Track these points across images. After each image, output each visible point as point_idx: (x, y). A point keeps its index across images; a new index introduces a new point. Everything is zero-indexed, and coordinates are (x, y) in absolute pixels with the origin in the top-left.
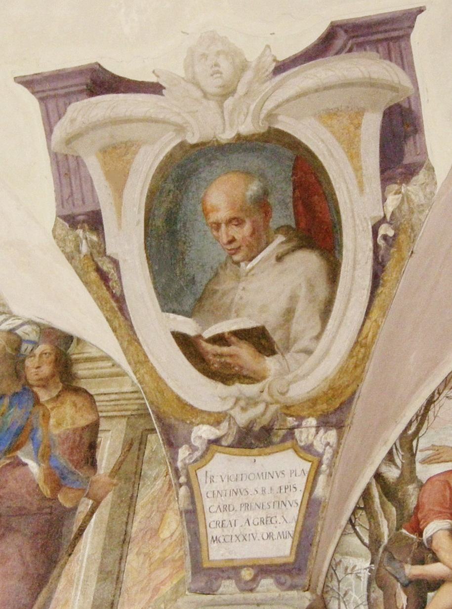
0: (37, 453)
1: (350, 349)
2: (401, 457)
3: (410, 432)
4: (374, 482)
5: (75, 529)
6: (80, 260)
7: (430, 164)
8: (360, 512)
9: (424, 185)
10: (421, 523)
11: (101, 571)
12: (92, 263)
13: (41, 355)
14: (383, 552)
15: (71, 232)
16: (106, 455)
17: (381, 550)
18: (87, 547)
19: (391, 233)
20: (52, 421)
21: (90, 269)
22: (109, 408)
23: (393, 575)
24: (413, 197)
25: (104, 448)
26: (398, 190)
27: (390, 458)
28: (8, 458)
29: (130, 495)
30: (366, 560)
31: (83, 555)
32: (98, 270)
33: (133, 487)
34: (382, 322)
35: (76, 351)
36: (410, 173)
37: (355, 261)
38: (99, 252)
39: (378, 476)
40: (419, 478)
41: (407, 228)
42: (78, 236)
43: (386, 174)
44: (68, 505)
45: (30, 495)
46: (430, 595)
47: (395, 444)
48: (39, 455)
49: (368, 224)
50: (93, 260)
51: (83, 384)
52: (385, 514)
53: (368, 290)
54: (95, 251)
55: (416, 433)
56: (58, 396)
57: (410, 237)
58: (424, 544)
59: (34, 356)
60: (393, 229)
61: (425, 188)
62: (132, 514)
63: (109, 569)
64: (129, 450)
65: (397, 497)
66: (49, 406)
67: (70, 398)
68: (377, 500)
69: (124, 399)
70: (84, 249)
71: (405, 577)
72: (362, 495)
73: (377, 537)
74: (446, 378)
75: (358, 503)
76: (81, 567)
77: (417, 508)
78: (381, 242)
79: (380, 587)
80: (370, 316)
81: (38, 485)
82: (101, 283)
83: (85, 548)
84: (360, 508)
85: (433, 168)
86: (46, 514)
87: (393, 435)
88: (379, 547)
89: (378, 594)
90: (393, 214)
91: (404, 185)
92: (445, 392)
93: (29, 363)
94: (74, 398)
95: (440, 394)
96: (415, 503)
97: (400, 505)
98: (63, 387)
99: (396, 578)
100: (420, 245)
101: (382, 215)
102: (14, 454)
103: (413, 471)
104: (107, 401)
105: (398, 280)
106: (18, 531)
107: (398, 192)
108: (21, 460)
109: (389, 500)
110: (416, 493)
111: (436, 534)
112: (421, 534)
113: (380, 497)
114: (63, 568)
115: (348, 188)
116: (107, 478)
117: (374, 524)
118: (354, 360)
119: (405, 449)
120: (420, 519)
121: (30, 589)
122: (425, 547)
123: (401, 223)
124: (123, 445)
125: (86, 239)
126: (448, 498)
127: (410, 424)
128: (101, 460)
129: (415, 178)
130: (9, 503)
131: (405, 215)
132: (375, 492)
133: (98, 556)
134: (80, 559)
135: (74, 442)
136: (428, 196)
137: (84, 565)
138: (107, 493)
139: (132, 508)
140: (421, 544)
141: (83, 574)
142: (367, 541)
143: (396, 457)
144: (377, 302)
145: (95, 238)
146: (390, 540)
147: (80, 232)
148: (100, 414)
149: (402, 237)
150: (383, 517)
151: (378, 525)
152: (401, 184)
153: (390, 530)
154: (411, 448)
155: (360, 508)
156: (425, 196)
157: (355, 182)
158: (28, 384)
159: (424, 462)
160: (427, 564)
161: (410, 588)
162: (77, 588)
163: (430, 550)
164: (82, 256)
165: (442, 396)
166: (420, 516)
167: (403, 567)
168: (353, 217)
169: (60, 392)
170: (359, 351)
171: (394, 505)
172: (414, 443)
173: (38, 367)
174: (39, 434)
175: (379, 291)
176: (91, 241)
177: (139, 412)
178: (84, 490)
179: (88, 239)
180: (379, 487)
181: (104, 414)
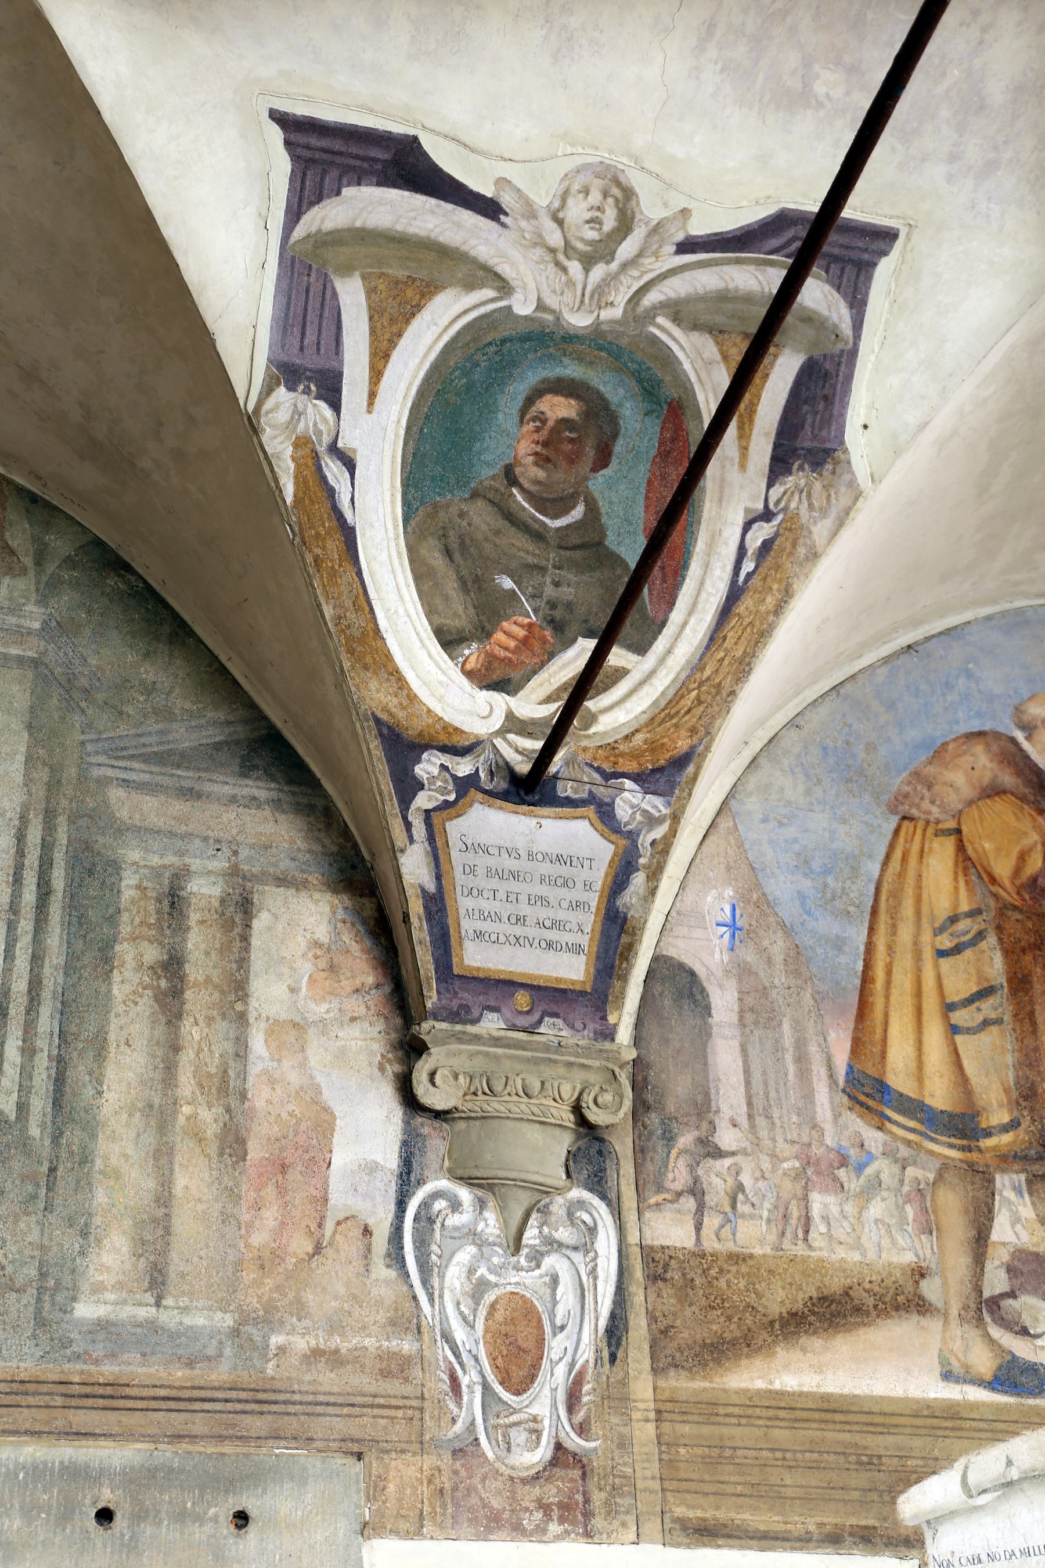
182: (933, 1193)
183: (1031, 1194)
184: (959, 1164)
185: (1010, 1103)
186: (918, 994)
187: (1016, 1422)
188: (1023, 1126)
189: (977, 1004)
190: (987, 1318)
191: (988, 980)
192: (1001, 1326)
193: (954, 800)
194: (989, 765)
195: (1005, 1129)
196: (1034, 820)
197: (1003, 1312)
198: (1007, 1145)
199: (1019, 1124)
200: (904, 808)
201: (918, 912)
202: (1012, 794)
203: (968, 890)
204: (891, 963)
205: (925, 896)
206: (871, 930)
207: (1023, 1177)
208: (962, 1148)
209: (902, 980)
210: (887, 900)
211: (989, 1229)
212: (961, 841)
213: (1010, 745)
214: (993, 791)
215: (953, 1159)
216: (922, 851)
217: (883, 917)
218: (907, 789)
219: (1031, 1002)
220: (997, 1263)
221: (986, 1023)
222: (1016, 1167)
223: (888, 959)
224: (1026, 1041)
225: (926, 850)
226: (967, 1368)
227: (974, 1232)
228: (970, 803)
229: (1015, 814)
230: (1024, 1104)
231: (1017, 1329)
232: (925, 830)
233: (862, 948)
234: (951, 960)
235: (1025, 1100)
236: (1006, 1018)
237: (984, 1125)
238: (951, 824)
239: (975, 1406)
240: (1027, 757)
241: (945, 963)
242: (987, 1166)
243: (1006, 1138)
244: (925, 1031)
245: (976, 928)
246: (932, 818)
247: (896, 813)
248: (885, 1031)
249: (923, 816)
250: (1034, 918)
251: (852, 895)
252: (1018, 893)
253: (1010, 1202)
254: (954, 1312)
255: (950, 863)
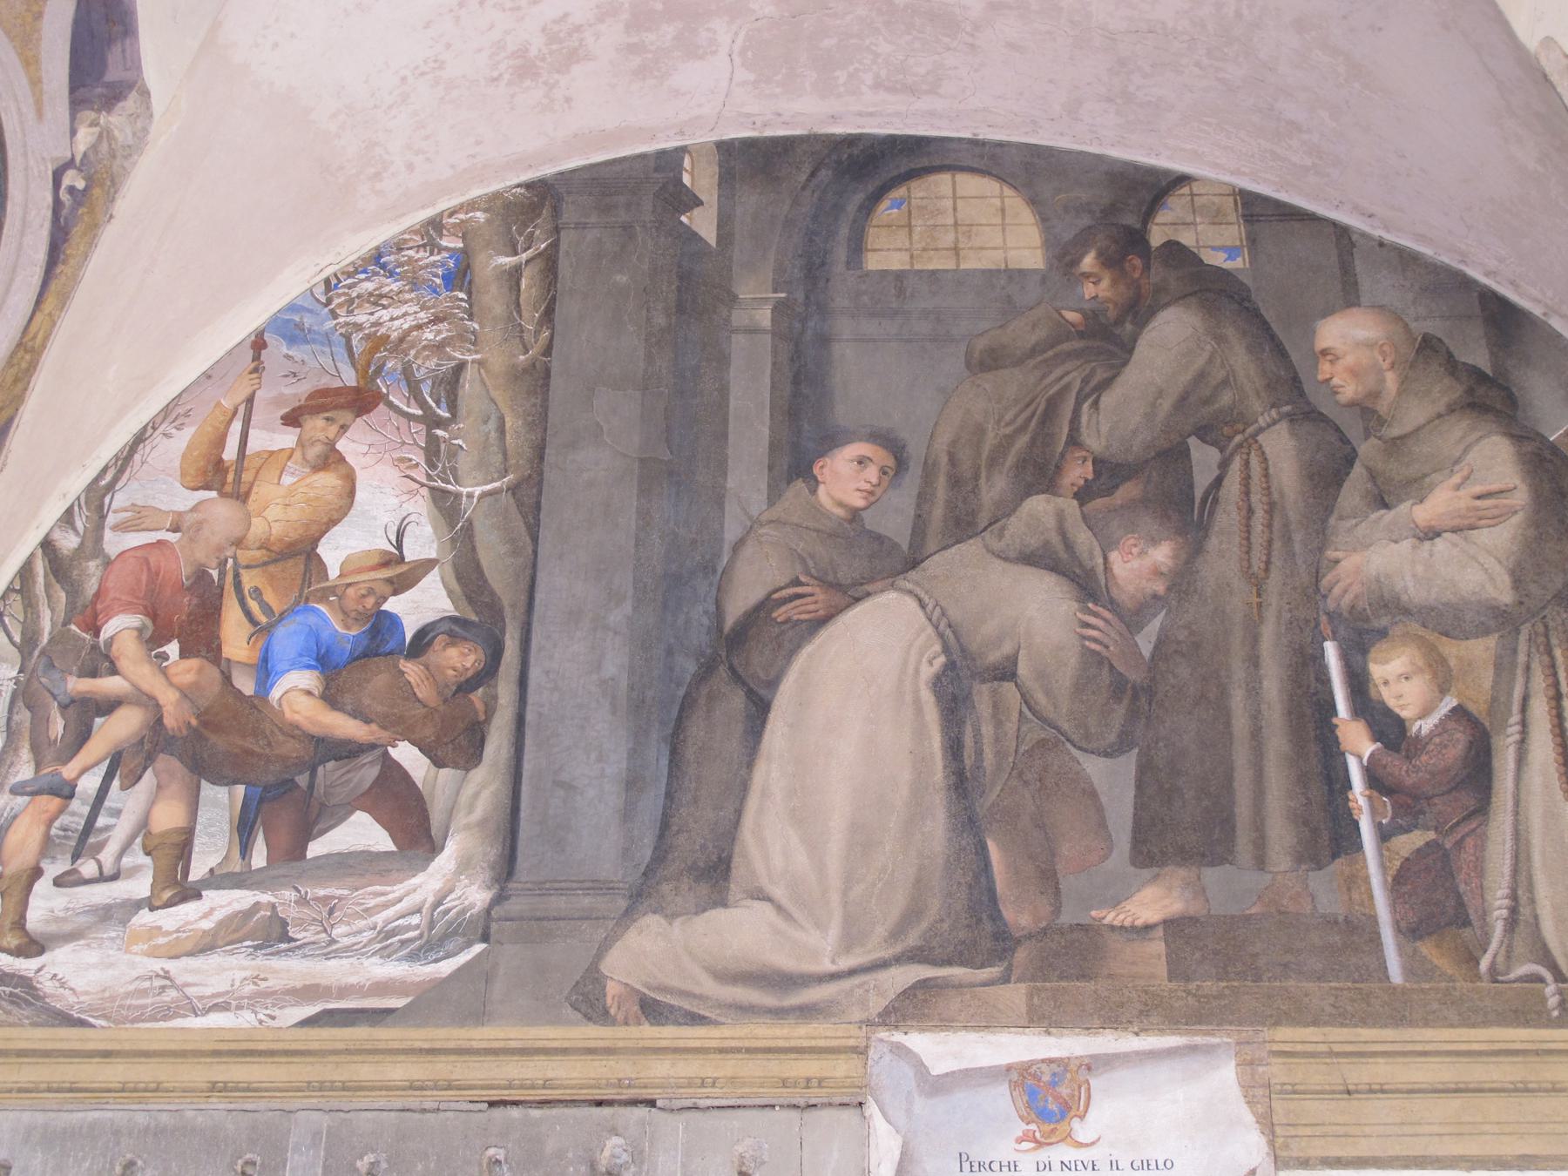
1: (9, 353)
2: (84, 520)
3: (103, 483)
4: (40, 551)
7: (144, 85)
8: (14, 596)
9: (134, 117)
10: (101, 616)
14: (39, 657)
17: (36, 653)
19: (80, 185)
23: (49, 691)
24: (116, 133)
26: (94, 120)
27: (68, 518)
30: (13, 667)
34: (59, 317)
36: (114, 96)
37: (25, 223)
39: (47, 545)
40: (106, 551)
41: (104, 179)
43: (77, 94)
46: (98, 721)
47: (78, 498)
49: (46, 167)
52: (49, 601)
53: (41, 267)
55: (111, 487)
57: (108, 193)
58: (100, 648)
60: (84, 178)
61: (136, 122)
65: (70, 577)
68: (41, 580)
71: (66, 692)
72: (19, 572)
73: (34, 634)
74: (168, 405)
75: (12, 582)
77: (97, 595)
78: (64, 196)
79: (29, 707)
80: (42, 306)
84: (14, 590)
85: (148, 93)
87: (76, 484)
88: (34, 649)
89: (23, 716)
90: (85, 155)
91: (104, 113)
92: (163, 426)
95: (154, 429)
96: (95, 587)
97: (74, 591)
99: (52, 694)
100: (127, 202)
101: (69, 155)
103: (99, 539)
105: (86, 256)
107: (94, 124)
109: (58, 582)
110: (99, 573)
111: (119, 635)
112: (97, 634)
113: (46, 576)
115: (19, 109)
117: (32, 613)
118: (13, 371)
119: (93, 508)
120: (99, 611)
122: (101, 652)
123: (96, 172)
126: (144, 583)
127: (105, 470)
129: (121, 104)
131: (103, 159)
132: (40, 567)
136: (138, 134)
140: (95, 647)
142: (17, 639)
143: (77, 518)
144: (54, 286)
146: (50, 641)
149: (97, 192)
150: (46, 606)
151: (37, 617)
152: (99, 111)
153: (53, 624)
154: (101, 506)
155: (14, 590)
156: (134, 134)
157: (31, 100)
159: (115, 528)
160: (101, 677)
161: (71, 710)
163: (107, 657)
165: (157, 432)
166: (99, 607)
167: (64, 680)
168: (25, 155)
170: (22, 358)
171: (63, 589)
172: (107, 500)
175: (58, 271)
180: (47, 562)
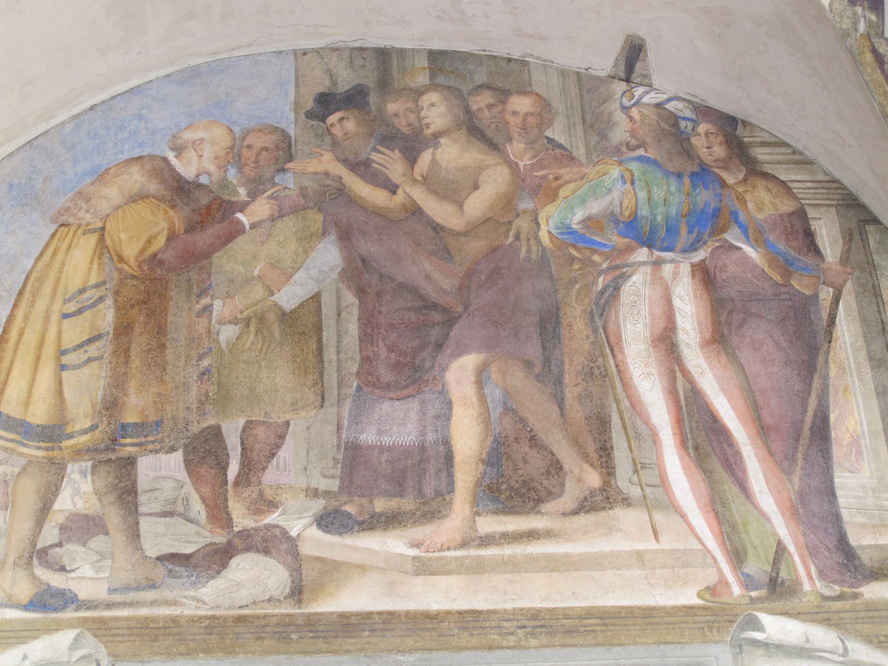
0: (747, 237)
5: (825, 314)
6: (856, 39)
11: (871, 359)
12: (868, 43)
13: (707, 134)
15: (849, 8)
16: (827, 244)
18: (846, 335)
20: (750, 205)
21: (866, 49)
22: (810, 196)
25: (822, 236)
28: (716, 241)
29: (871, 284)
31: (845, 343)
32: (874, 51)
33: (871, 276)
35: (745, 134)
38: (877, 34)
42: (855, 14)
44: (807, 292)
45: (758, 280)
48: (751, 240)
50: (870, 41)
51: (768, 169)
54: (872, 32)
56: (745, 180)
59: (699, 135)
62: (881, 303)
63: (879, 356)
64: (851, 240)
66: (740, 190)
67: (761, 183)
69: (823, 188)
70: (862, 27)
76: (847, 354)
81: (763, 270)
82: (876, 65)
83: (843, 336)
86: (786, 300)
93: (694, 141)
94: (764, 183)
98: (747, 171)
102: (721, 237)
104: (804, 189)
106: (760, 316)
108: (732, 244)
114: (827, 353)
116: (839, 267)
121: (799, 375)
124: (842, 234)
125: (865, 17)
128: (825, 249)
130: (738, 288)
133: (861, 342)
134: (843, 346)
135: (786, 228)
137: (850, 351)
138: (846, 281)
139: (879, 298)
141: (852, 360)
145: (874, 18)
147: (859, 9)
148: (803, 202)
158: (705, 164)
162: (852, 375)
164: (858, 35)
169: (745, 175)
173: (708, 148)
174: (742, 217)
176: (870, 21)
177: (845, 202)
178: (819, 277)
179: (867, 18)
181: (807, 202)
182: (16, 481)
183: (93, 474)
184: (41, 460)
185: (94, 414)
186: (41, 346)
187: (39, 630)
188: (100, 428)
189: (86, 348)
190: (35, 561)
191: (98, 331)
192: (45, 567)
193: (104, 207)
194: (140, 179)
195: (85, 432)
196: (166, 213)
197: (49, 557)
198: (82, 443)
199: (97, 428)
200: (63, 219)
201: (55, 290)
202: (154, 197)
203: (99, 269)
204: (24, 328)
205: (63, 278)
206: (15, 306)
207: (90, 464)
208: (47, 449)
209: (31, 339)
210: (33, 284)
211: (53, 502)
212: (103, 235)
213: (162, 165)
214: (141, 197)
215: (37, 457)
216: (70, 246)
217: (27, 296)
218: (69, 204)
219: (130, 342)
220: (53, 524)
221: (90, 360)
222: (86, 457)
223: (24, 324)
224: (118, 369)
225: (73, 246)
226: (10, 597)
227: (41, 505)
228: (118, 208)
229: (152, 211)
230: (104, 413)
231: (57, 567)
232: (76, 232)
233: (4, 319)
234: (73, 319)
235: (107, 409)
236: (106, 355)
237: (68, 431)
238: (99, 224)
239: (10, 622)
240: (173, 170)
241: (67, 323)
242: (63, 459)
243: (84, 438)
244: (40, 372)
245: (98, 295)
246: (84, 223)
247: (57, 223)
248: (8, 375)
249: (77, 222)
250: (147, 282)
251: (6, 284)
252: (139, 266)
253: (75, 482)
254: (11, 560)
255: (90, 252)
